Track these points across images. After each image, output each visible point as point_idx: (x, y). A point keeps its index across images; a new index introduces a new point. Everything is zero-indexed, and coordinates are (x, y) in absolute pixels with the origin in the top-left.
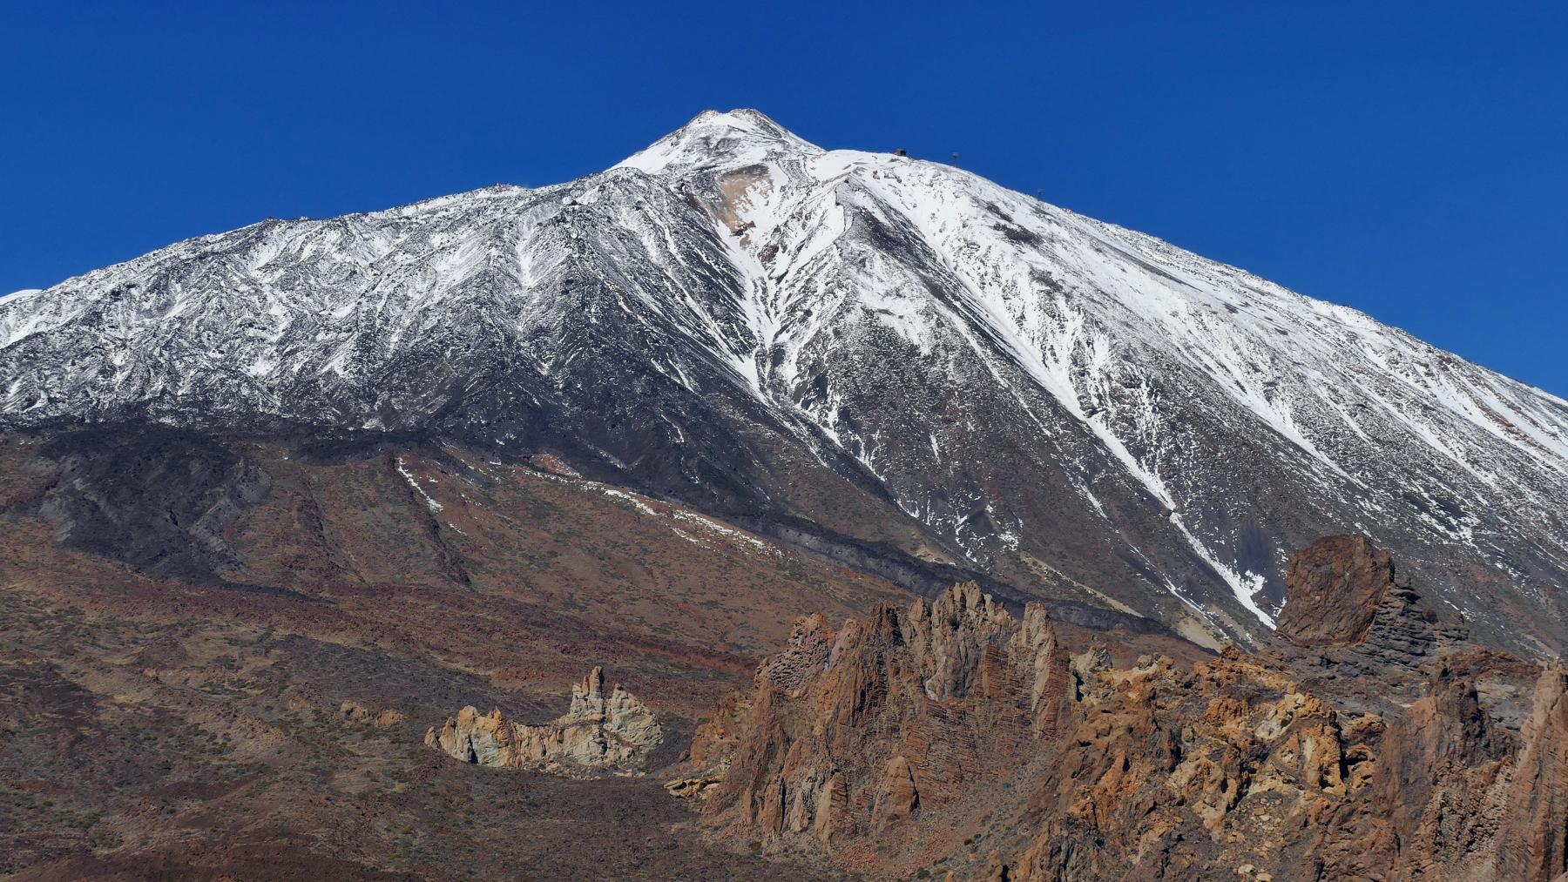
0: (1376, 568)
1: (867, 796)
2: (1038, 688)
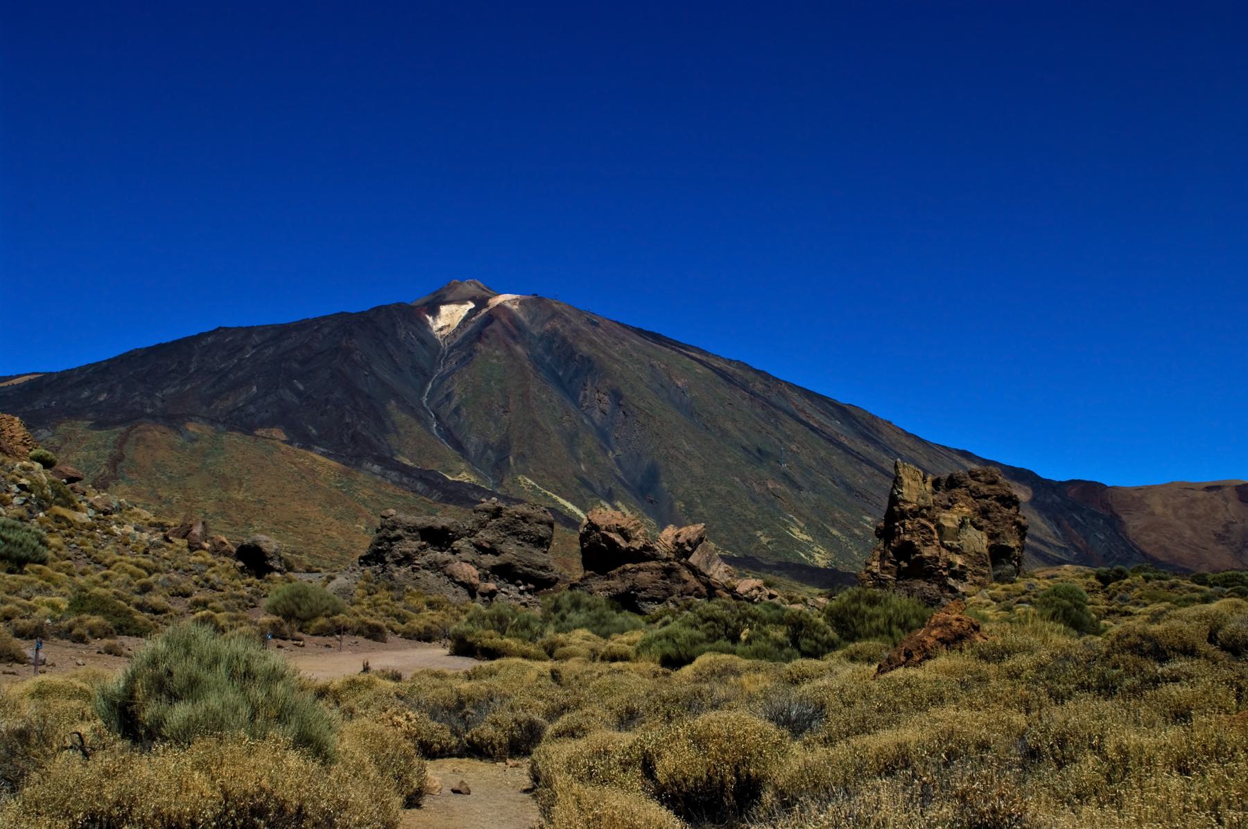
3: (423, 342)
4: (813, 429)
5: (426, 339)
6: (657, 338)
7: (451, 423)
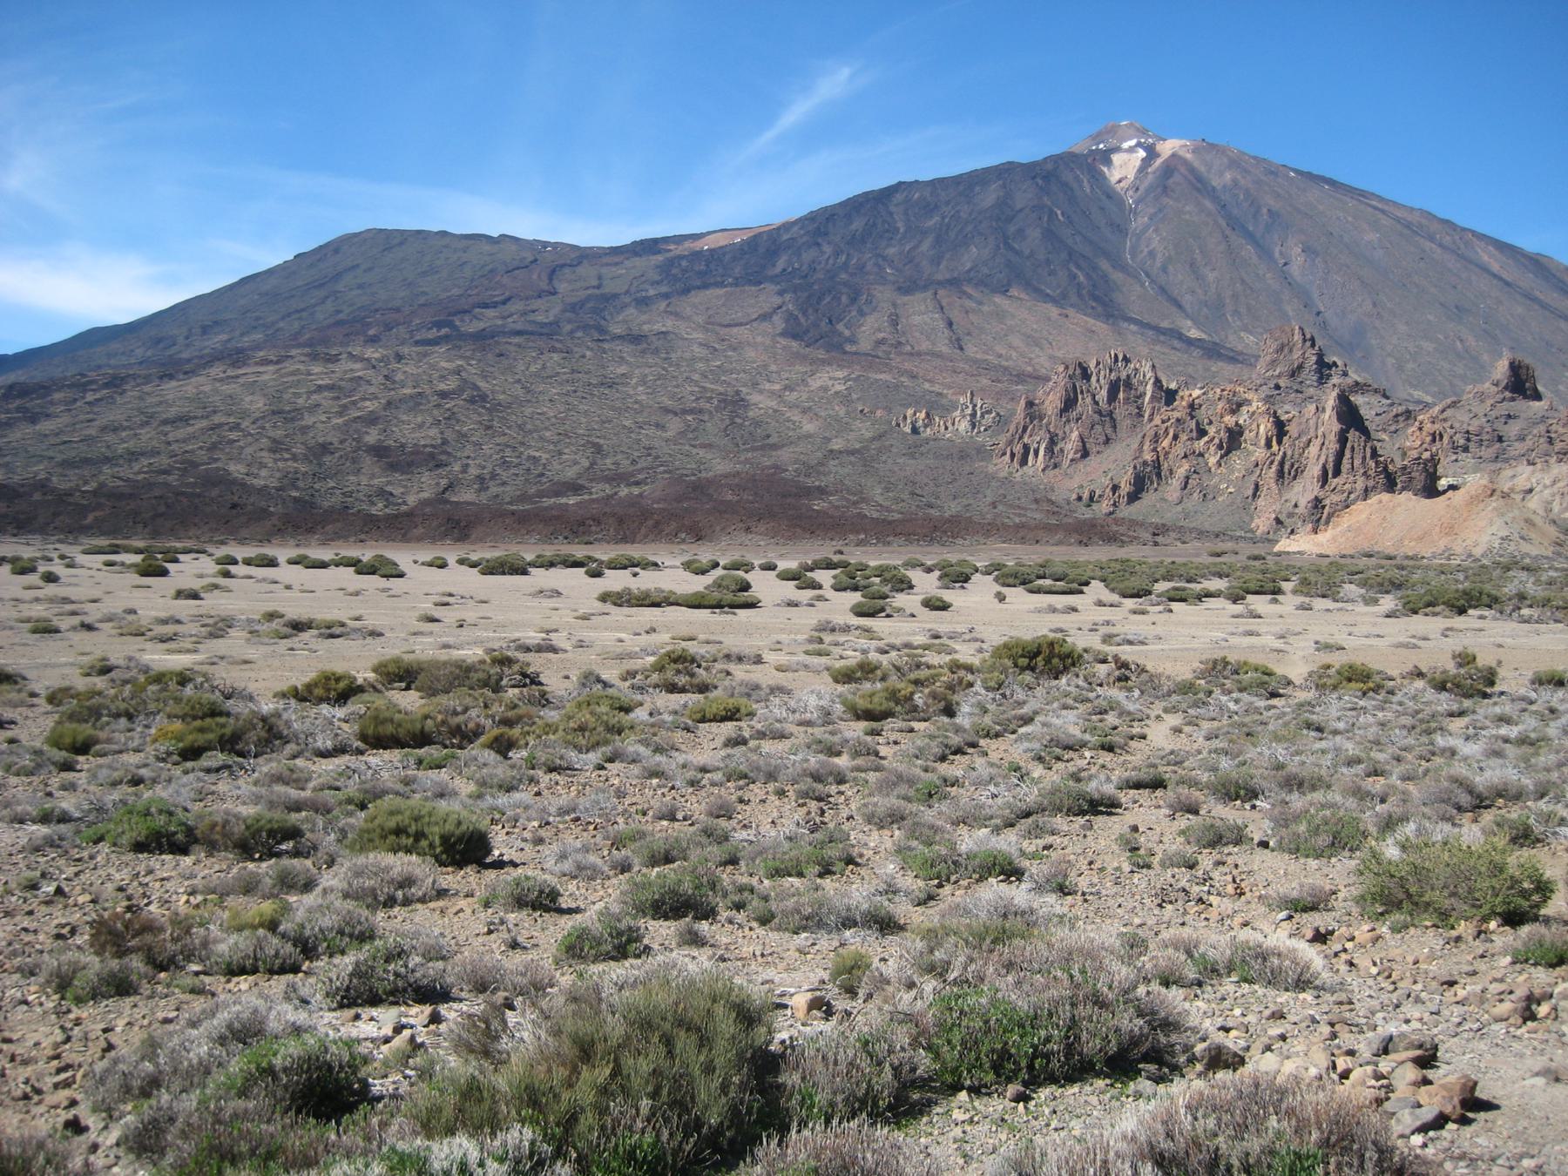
0: (1305, 340)
1: (1062, 450)
2: (1147, 399)
3: (1109, 197)
4: (1507, 284)
5: (1110, 194)
6: (1332, 183)
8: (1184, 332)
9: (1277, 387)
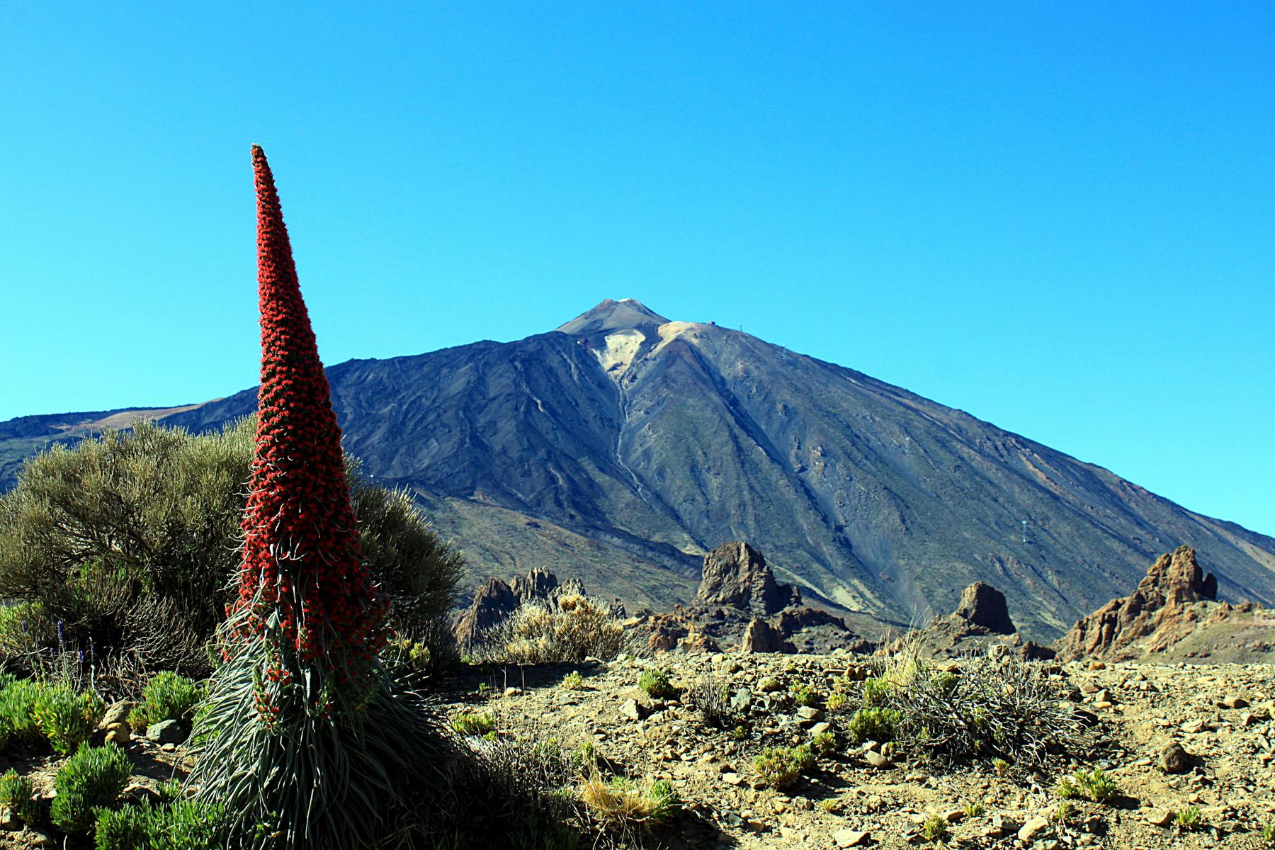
4: (1056, 498)
5: (603, 383)
6: (861, 377)
7: (658, 485)
8: (678, 546)
9: (720, 615)
